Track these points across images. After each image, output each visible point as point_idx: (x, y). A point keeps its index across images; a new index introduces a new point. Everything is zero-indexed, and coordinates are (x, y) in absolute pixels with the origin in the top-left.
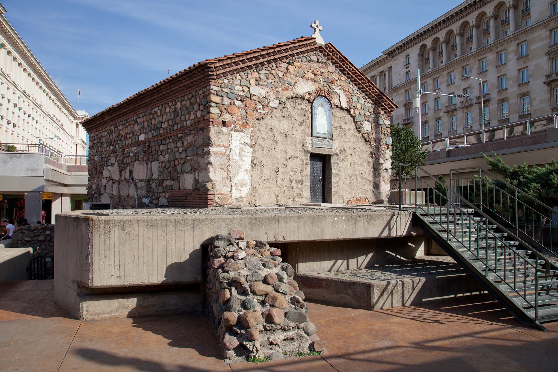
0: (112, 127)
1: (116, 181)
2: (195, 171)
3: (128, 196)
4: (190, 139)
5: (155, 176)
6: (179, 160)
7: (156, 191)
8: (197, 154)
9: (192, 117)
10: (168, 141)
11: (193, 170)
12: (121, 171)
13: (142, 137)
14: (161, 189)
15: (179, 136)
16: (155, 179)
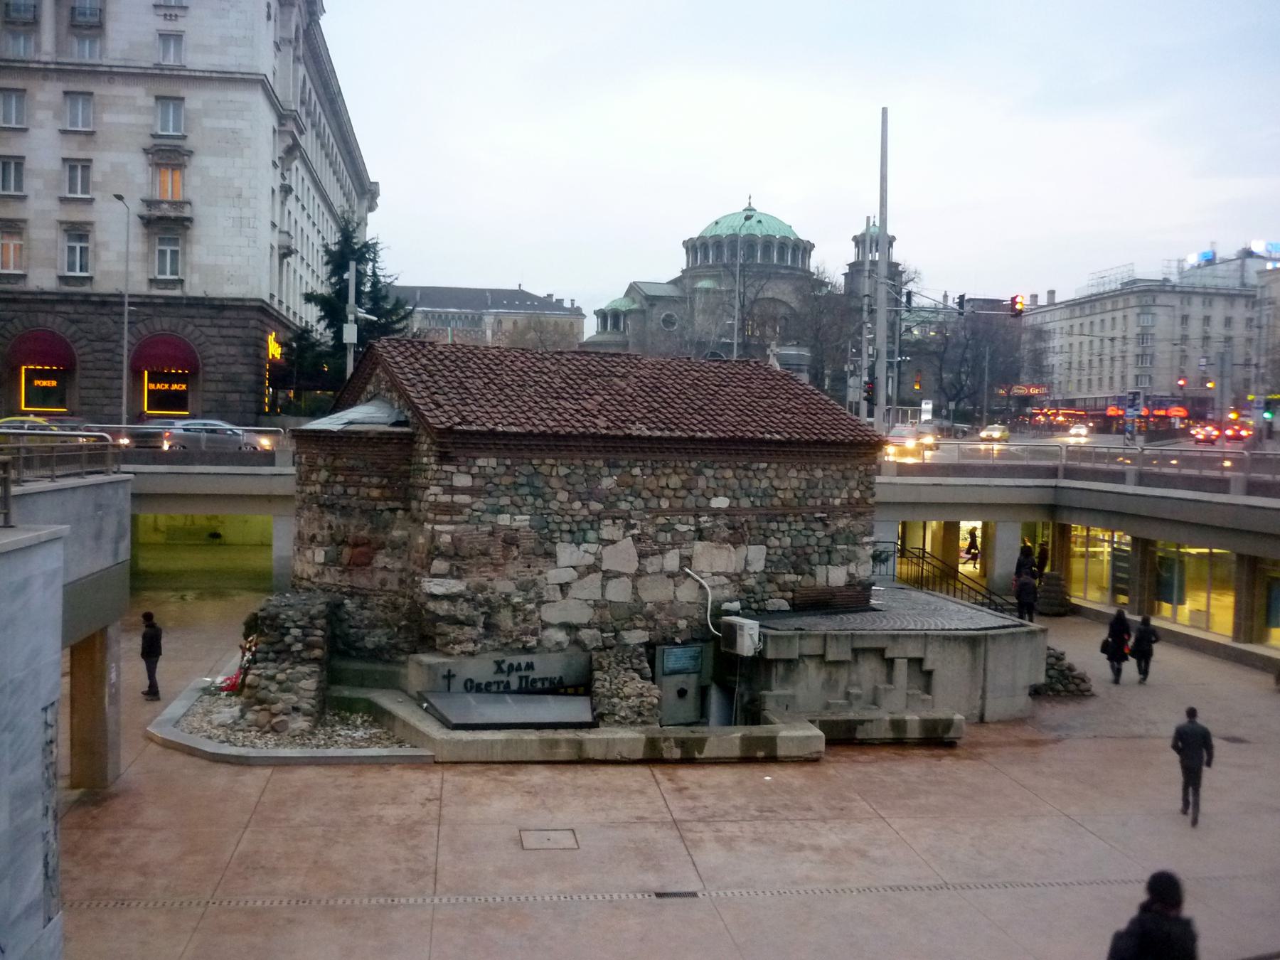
0: (600, 463)
1: (619, 575)
2: (848, 564)
3: (672, 602)
4: (841, 523)
5: (758, 565)
6: (816, 548)
7: (758, 589)
8: (856, 544)
9: (845, 495)
10: (791, 519)
11: (846, 561)
12: (642, 556)
13: (721, 502)
14: (771, 587)
15: (818, 515)
16: (755, 573)
